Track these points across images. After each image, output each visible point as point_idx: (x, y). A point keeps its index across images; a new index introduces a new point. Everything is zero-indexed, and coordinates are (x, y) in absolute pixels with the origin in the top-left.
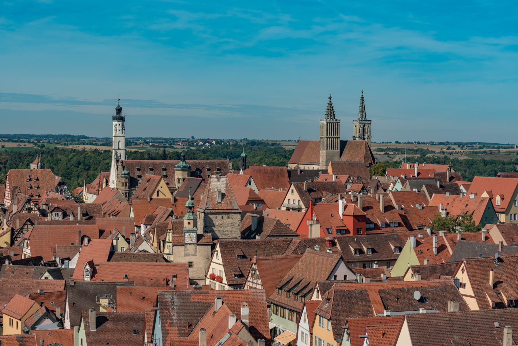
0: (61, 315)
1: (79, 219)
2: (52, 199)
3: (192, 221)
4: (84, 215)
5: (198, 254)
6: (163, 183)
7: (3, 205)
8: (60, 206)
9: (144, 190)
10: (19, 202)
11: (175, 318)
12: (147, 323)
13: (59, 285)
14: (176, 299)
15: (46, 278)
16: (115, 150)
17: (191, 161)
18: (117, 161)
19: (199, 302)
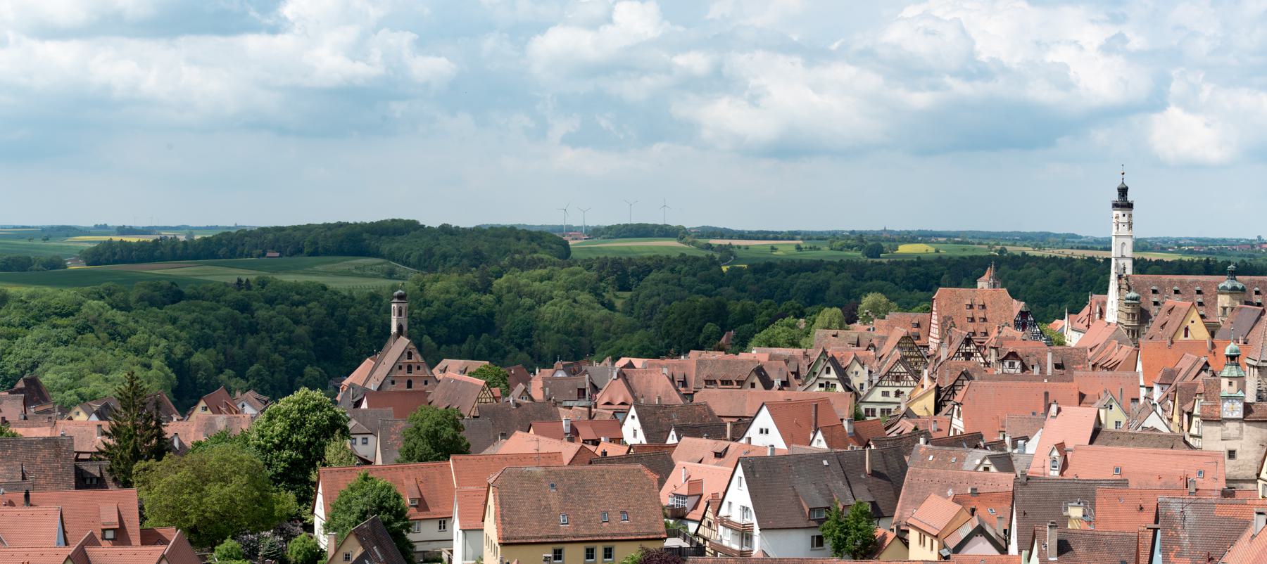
0: (1005, 531)
1: (1049, 370)
2: (1007, 338)
3: (1235, 383)
4: (1058, 366)
5: (1245, 436)
6: (1195, 315)
7: (927, 347)
8: (1019, 351)
9: (1162, 327)
10: (950, 343)
11: (1186, 542)
12: (1141, 551)
13: (1005, 481)
14: (1188, 511)
15: (986, 469)
16: (1117, 259)
17: (1246, 278)
18: (1120, 277)
19: (1229, 519)
